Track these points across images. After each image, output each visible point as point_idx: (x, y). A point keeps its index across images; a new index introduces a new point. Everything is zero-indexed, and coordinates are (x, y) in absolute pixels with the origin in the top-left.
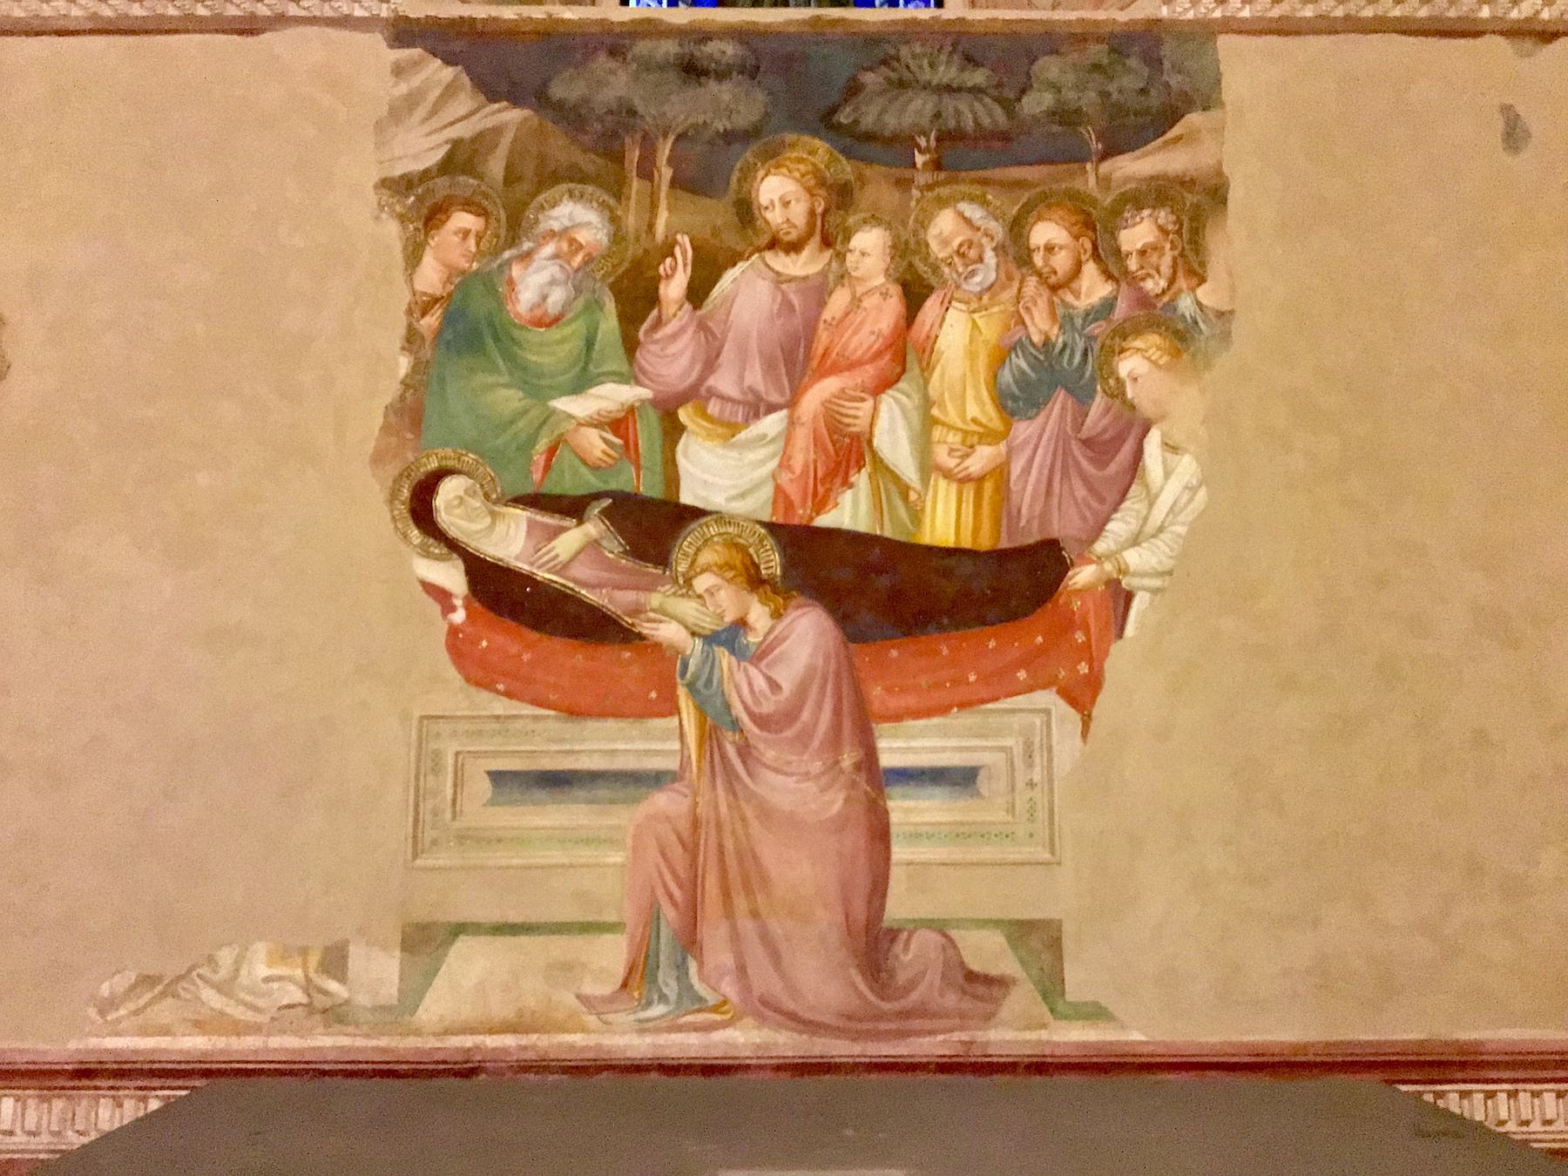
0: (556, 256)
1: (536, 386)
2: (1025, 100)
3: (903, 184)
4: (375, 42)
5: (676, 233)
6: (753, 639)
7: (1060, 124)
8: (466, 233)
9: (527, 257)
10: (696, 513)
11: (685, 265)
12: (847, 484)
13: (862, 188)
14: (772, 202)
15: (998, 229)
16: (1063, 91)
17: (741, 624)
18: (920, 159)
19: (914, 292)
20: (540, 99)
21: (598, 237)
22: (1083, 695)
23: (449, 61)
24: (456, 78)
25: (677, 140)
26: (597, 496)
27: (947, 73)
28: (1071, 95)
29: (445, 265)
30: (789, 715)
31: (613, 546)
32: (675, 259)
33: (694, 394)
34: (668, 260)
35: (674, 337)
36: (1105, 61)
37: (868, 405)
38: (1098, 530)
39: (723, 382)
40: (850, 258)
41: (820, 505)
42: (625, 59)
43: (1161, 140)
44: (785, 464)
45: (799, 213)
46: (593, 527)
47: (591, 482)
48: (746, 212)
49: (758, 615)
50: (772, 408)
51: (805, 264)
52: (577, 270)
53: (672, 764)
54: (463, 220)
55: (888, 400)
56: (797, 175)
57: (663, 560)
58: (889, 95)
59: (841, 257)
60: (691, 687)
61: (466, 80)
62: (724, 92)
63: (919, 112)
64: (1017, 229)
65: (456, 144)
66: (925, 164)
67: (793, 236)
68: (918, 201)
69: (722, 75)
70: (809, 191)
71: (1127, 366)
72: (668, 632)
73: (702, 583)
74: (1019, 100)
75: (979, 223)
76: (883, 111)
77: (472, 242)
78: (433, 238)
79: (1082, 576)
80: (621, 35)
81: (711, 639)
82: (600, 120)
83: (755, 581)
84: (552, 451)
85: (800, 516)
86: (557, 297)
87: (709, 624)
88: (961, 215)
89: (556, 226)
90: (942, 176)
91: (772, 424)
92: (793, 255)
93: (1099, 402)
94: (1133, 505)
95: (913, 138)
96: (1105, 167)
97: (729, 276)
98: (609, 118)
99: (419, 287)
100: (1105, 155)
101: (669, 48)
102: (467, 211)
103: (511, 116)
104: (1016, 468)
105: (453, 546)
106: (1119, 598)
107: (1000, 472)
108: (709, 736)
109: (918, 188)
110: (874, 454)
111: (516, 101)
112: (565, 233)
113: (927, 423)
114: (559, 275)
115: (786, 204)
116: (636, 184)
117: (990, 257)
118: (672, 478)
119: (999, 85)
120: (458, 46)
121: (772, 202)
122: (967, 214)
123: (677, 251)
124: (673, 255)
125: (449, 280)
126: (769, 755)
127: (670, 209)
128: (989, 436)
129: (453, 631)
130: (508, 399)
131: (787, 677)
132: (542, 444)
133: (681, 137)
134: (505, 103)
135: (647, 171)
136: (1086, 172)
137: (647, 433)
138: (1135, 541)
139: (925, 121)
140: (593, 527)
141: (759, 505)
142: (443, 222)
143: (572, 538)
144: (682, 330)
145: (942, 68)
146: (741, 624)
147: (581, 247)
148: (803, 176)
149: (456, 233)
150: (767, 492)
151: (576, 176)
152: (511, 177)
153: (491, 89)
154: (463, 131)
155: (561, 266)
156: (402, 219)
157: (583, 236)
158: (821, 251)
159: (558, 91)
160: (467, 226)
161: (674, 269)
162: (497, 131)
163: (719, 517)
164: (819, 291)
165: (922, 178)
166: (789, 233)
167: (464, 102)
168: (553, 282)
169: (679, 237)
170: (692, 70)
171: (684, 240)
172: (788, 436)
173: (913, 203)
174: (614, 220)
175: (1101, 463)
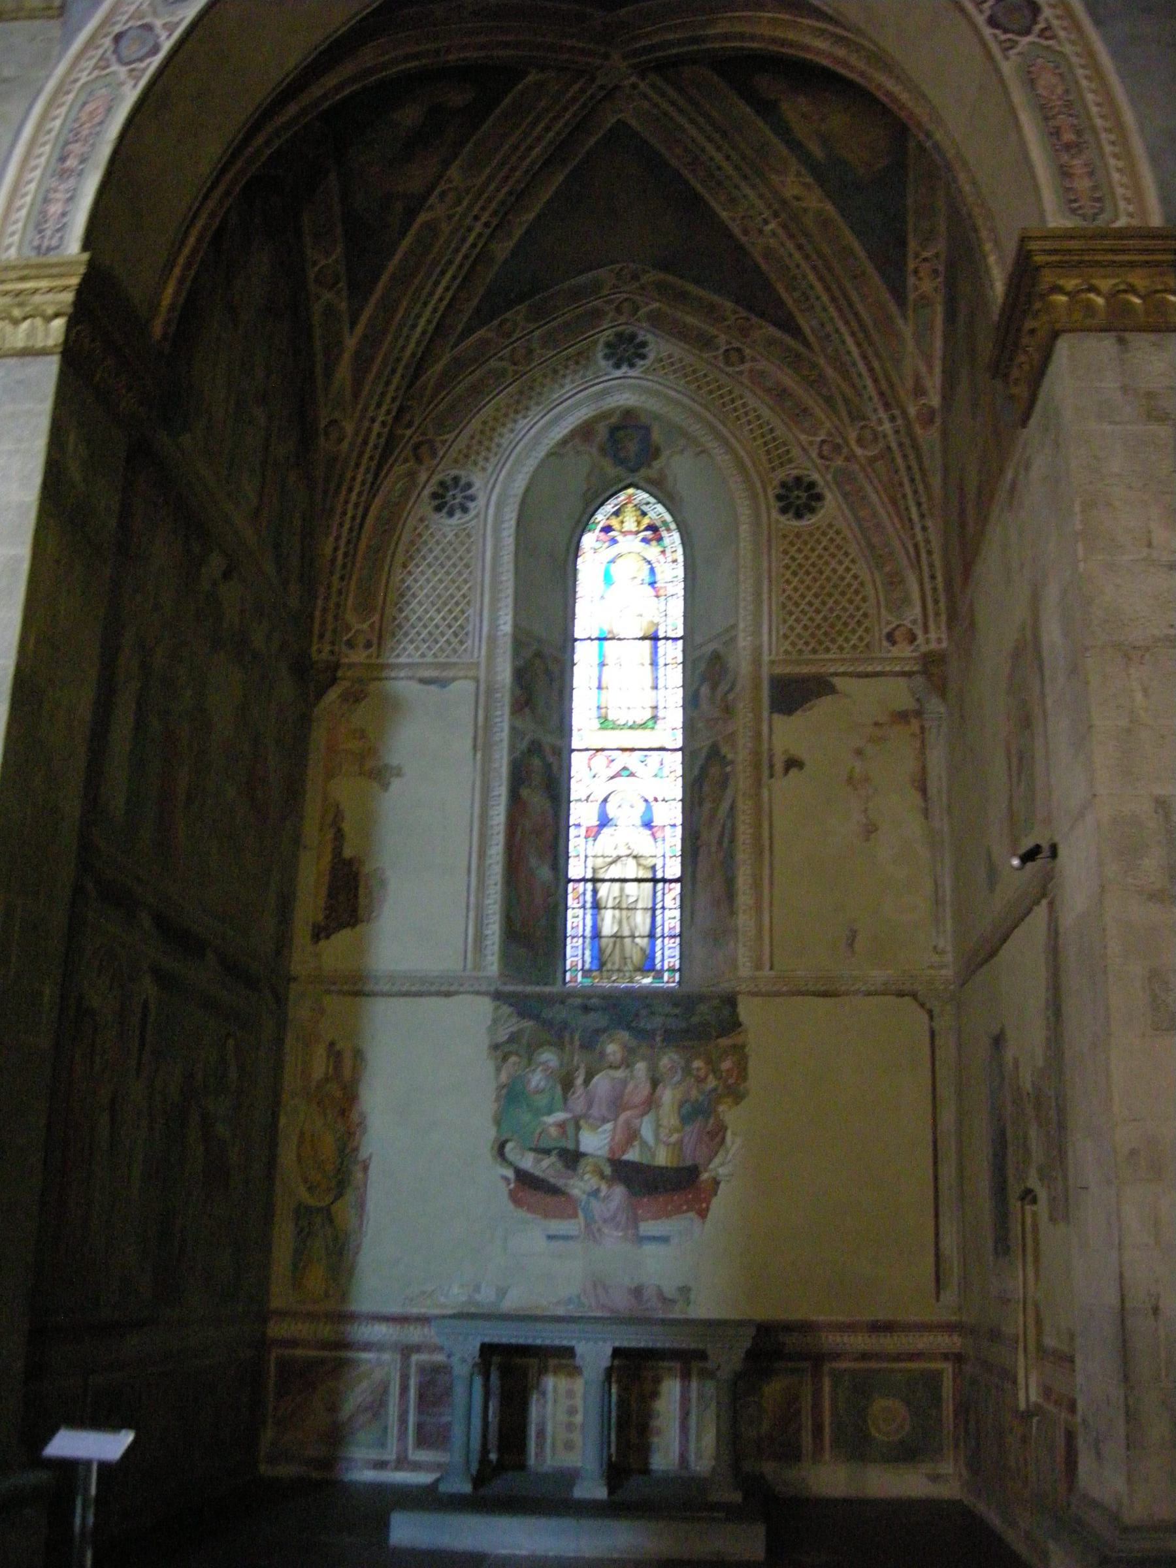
0: (542, 1071)
1: (538, 1113)
3: (652, 1047)
6: (602, 1194)
9: (534, 1070)
10: (584, 1155)
12: (632, 1146)
15: (683, 1063)
17: (598, 1190)
19: (655, 1083)
20: (536, 1017)
22: (703, 1214)
23: (511, 1005)
26: (555, 1148)
30: (614, 1218)
31: (559, 1165)
33: (586, 1116)
35: (579, 1098)
37: (639, 1120)
38: (711, 1160)
39: (594, 1112)
40: (635, 1072)
41: (624, 1152)
44: (613, 1139)
45: (619, 1056)
46: (553, 1158)
47: (552, 1144)
48: (602, 1054)
49: (604, 1187)
50: (608, 1121)
51: (619, 1074)
53: (576, 1233)
54: (513, 1059)
55: (646, 1119)
57: (574, 1169)
59: (632, 1072)
60: (583, 1209)
64: (688, 1062)
65: (512, 1034)
71: (721, 1108)
72: (576, 1192)
73: (587, 1177)
79: (705, 1176)
81: (589, 1195)
83: (602, 1176)
84: (540, 1134)
85: (617, 1157)
86: (542, 1084)
87: (588, 1189)
91: (608, 1126)
93: (711, 1121)
94: (721, 1153)
97: (597, 1077)
100: (717, 1037)
103: (528, 1024)
104: (686, 1140)
105: (510, 1164)
106: (716, 1183)
107: (680, 1142)
108: (587, 1226)
110: (641, 1137)
113: (658, 1126)
117: (680, 1072)
118: (577, 1142)
126: (606, 1231)
128: (677, 1131)
129: (510, 1190)
130: (527, 1117)
131: (613, 1205)
132: (538, 1131)
135: (572, 1042)
137: (570, 1129)
138: (722, 1164)
139: (660, 1025)
140: (553, 1158)
141: (604, 1152)
143: (546, 1162)
144: (581, 1095)
146: (598, 1190)
150: (607, 1148)
151: (550, 1044)
153: (522, 1014)
154: (514, 1029)
156: (496, 1059)
157: (551, 1064)
163: (592, 1156)
164: (625, 1083)
167: (514, 1020)
168: (541, 1080)
170: (586, 1009)
172: (615, 1128)
175: (712, 1140)
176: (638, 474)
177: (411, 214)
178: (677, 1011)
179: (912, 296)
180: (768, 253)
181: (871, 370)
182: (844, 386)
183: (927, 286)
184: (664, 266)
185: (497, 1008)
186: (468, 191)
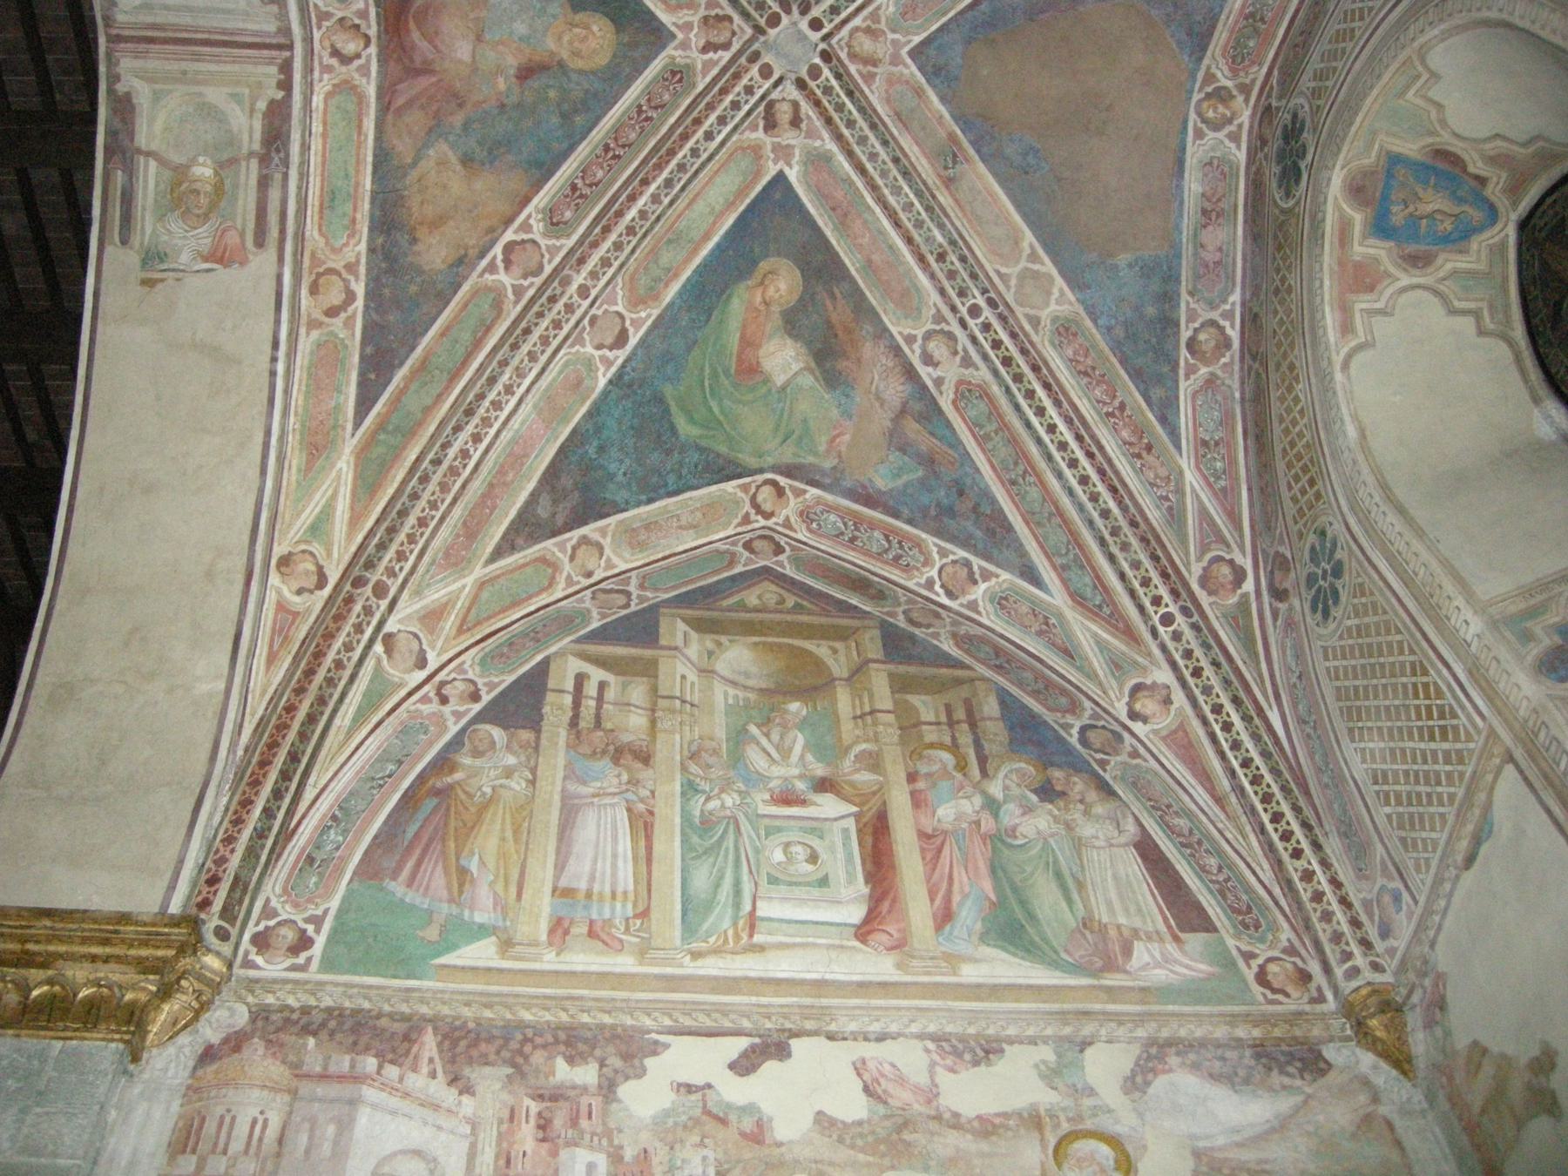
177: (930, 412)
184: (1199, 41)
186: (939, 318)
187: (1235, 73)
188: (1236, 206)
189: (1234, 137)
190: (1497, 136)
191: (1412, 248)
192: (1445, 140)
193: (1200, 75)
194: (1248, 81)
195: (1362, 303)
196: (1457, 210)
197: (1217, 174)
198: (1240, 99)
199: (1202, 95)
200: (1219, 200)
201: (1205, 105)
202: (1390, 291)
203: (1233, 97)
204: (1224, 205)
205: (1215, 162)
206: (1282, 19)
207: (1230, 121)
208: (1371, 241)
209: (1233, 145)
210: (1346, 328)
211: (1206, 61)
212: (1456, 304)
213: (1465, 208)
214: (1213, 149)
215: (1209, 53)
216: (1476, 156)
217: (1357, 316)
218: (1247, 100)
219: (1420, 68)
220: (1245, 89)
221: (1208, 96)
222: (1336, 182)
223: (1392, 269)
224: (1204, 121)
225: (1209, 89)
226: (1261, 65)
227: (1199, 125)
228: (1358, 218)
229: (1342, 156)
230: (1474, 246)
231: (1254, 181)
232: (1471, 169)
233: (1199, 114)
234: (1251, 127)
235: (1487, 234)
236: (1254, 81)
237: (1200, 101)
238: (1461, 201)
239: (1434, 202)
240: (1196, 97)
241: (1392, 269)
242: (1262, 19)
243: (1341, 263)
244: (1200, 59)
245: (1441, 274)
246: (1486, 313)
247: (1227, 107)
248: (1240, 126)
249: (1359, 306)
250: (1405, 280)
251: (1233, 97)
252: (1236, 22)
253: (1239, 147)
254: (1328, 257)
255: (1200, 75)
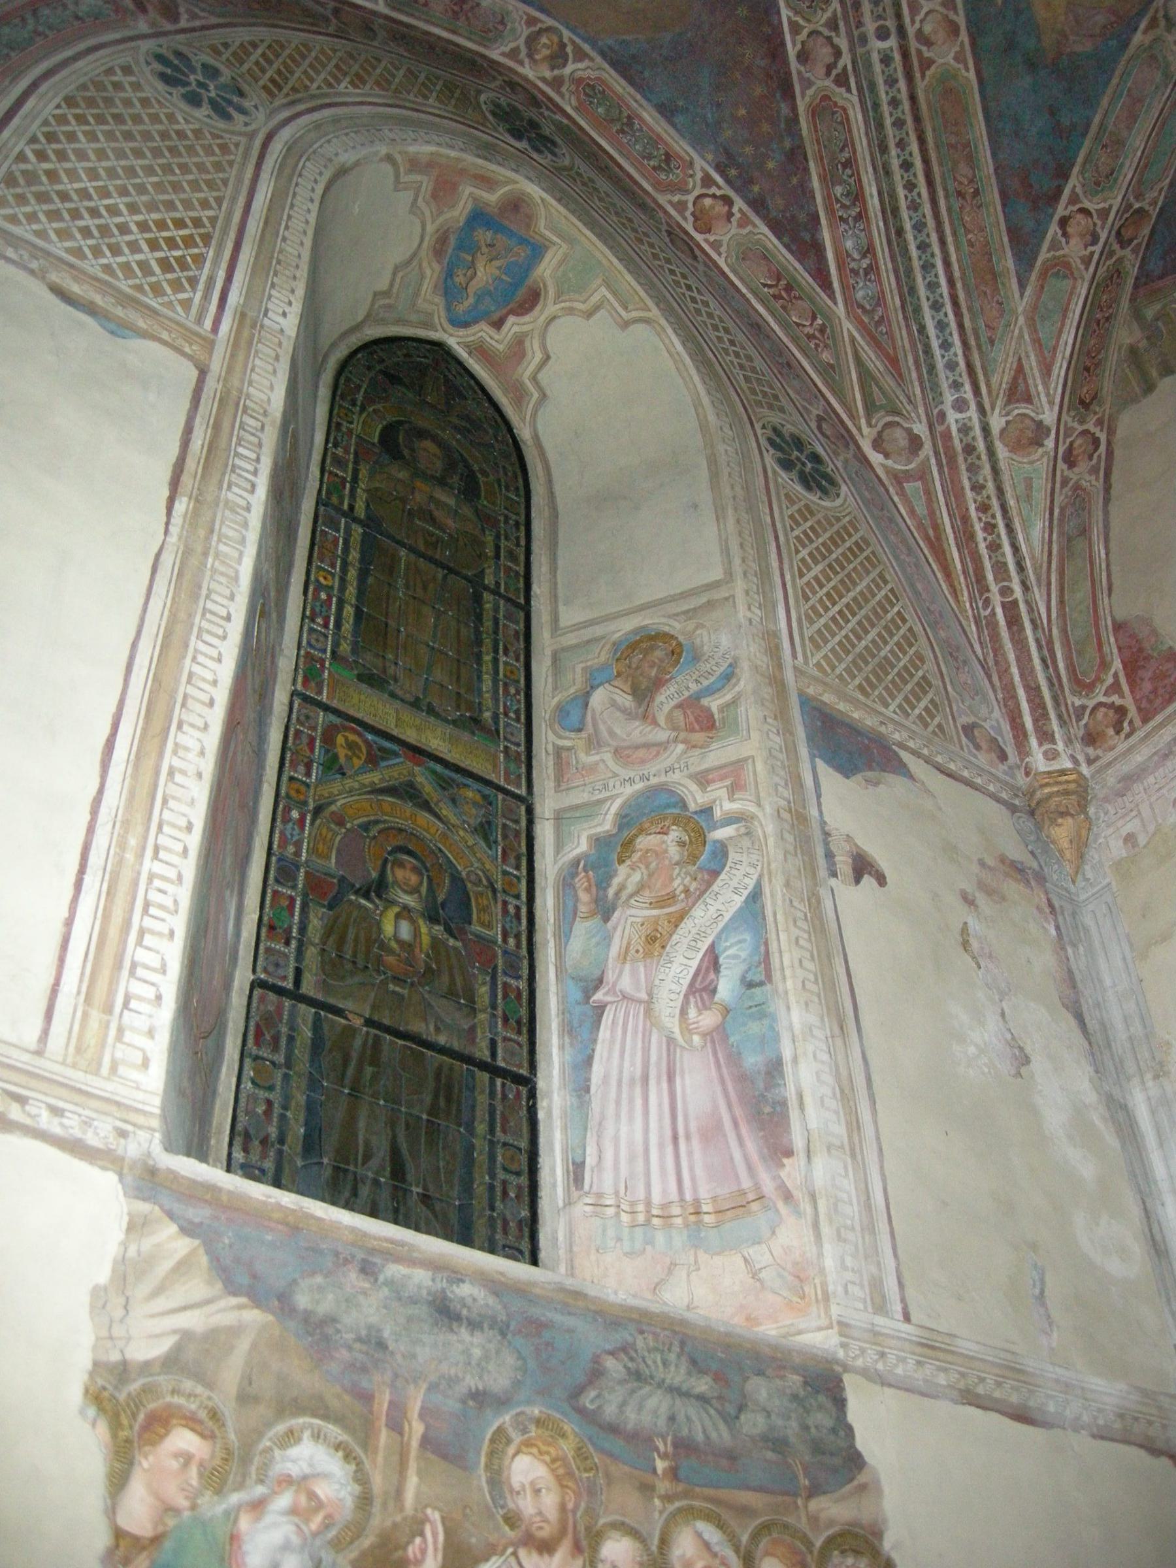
0: (293, 1511)
2: (742, 1417)
4: (107, 1182)
5: (426, 1506)
7: (773, 1450)
8: (187, 1459)
9: (258, 1506)
11: (436, 1549)
13: (609, 1484)
14: (523, 1486)
16: (773, 1417)
18: (660, 1465)
21: (343, 1494)
23: (188, 1229)
24: (193, 1253)
25: (429, 1389)
27: (678, 1375)
28: (780, 1422)
29: (157, 1496)
32: (425, 1541)
34: (418, 1540)
36: (802, 1393)
42: (376, 1280)
43: (848, 1487)
45: (550, 1501)
52: (315, 1535)
54: (183, 1440)
56: (547, 1458)
58: (629, 1386)
61: (204, 1260)
62: (475, 1343)
63: (655, 1412)
65: (186, 1336)
66: (665, 1470)
67: (545, 1533)
68: (661, 1512)
69: (474, 1325)
70: (559, 1479)
74: (737, 1418)
75: (717, 1549)
76: (623, 1404)
77: (193, 1471)
78: (146, 1458)
80: (372, 1251)
82: (350, 1348)
88: (699, 1535)
89: (294, 1470)
90: (680, 1487)
92: (546, 1556)
95: (649, 1440)
96: (814, 1505)
98: (357, 1346)
99: (124, 1522)
101: (421, 1276)
102: (193, 1430)
103: (254, 1316)
109: (660, 1497)
111: (257, 1301)
112: (301, 1483)
114: (295, 1540)
115: (537, 1492)
116: (384, 1437)
119: (720, 1398)
120: (198, 1214)
121: (523, 1486)
122: (706, 1536)
123: (428, 1530)
124: (422, 1534)
125: (159, 1521)
127: (419, 1473)
133: (432, 1388)
134: (243, 1300)
136: (797, 1507)
139: (662, 1422)
142: (162, 1437)
145: (673, 1368)
147: (320, 1505)
148: (554, 1461)
149: (176, 1455)
152: (245, 1398)
154: (194, 1321)
155: (298, 1526)
157: (323, 1490)
158: (573, 1556)
159: (303, 1301)
160: (192, 1450)
161: (423, 1551)
162: (235, 1331)
165: (663, 1486)
166: (541, 1528)
167: (197, 1287)
168: (286, 1547)
169: (429, 1511)
171: (435, 1516)
173: (656, 1515)
174: (361, 1478)
176: (462, 332)
178: (703, 1385)
179: (1044, 255)
180: (824, 108)
181: (961, 326)
182: (869, 355)
183: (1074, 249)
185: (136, 1226)
187: (579, 81)
188: (454, 32)
189: (513, 54)
190: (547, 358)
191: (452, 240)
192: (548, 307)
193: (586, 47)
194: (564, 89)
195: (426, 183)
196: (471, 290)
197: (490, 26)
198: (548, 74)
199: (566, 40)
200: (468, 19)
201: (556, 39)
202: (427, 214)
203: (553, 68)
204: (461, 23)
205: (500, 27)
206: (621, 153)
207: (530, 55)
208: (469, 206)
209: (507, 49)
210: (415, 165)
211: (599, 59)
212: (400, 274)
213: (471, 300)
214: (513, 30)
215: (606, 66)
216: (525, 328)
217: (419, 178)
218: (544, 80)
219: (635, 314)
220: (557, 83)
221: (562, 46)
222: (534, 190)
223: (441, 219)
224: (540, 32)
225: (569, 49)
226: (576, 109)
227: (539, 25)
228: (492, 198)
229: (554, 202)
230: (437, 300)
231: (473, 63)
232: (511, 319)
233: (549, 29)
234: (516, 73)
235: (443, 314)
236: (562, 96)
237: (561, 37)
238: (479, 298)
239: (485, 273)
240: (566, 34)
241: (441, 219)
242: (622, 131)
243: (462, 172)
244: (603, 54)
245: (425, 264)
246: (387, 301)
247: (545, 59)
248: (521, 63)
249: (425, 179)
250: (430, 228)
251: (553, 68)
252: (629, 107)
253: (503, 54)
254: (471, 160)
255: (586, 47)
